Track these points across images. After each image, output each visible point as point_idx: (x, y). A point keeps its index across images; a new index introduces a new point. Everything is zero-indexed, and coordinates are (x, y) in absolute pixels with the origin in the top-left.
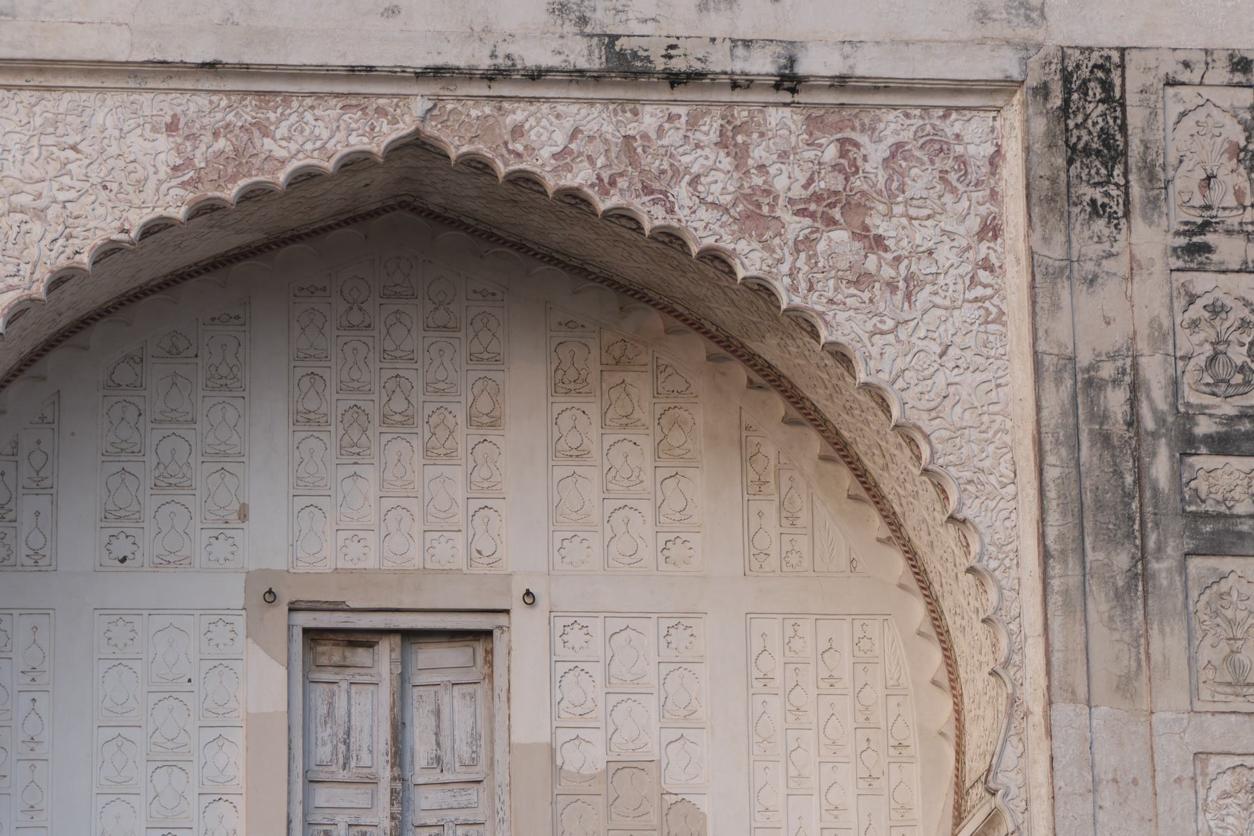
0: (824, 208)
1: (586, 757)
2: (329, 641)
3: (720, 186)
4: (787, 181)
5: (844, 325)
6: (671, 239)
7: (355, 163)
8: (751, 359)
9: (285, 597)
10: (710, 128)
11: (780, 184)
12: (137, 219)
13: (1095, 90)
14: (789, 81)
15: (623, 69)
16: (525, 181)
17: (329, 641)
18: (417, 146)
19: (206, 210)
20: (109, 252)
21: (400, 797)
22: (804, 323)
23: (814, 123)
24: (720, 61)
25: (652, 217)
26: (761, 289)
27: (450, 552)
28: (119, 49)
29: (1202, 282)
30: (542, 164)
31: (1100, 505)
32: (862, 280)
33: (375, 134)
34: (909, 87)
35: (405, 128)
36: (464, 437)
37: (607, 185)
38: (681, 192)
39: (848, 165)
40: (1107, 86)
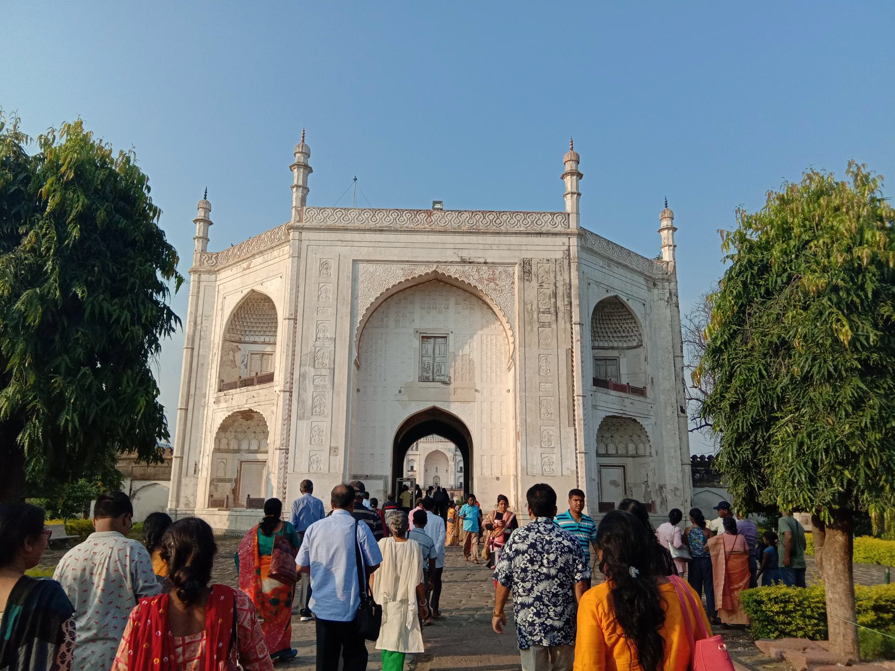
0: (492, 280)
2: (425, 338)
3: (476, 277)
6: (470, 284)
7: (427, 274)
10: (475, 268)
14: (486, 263)
15: (463, 262)
16: (450, 276)
17: (425, 338)
18: (435, 271)
20: (394, 286)
21: (434, 359)
24: (476, 260)
25: (467, 281)
28: (395, 259)
34: (502, 264)
36: (444, 310)
39: (494, 274)
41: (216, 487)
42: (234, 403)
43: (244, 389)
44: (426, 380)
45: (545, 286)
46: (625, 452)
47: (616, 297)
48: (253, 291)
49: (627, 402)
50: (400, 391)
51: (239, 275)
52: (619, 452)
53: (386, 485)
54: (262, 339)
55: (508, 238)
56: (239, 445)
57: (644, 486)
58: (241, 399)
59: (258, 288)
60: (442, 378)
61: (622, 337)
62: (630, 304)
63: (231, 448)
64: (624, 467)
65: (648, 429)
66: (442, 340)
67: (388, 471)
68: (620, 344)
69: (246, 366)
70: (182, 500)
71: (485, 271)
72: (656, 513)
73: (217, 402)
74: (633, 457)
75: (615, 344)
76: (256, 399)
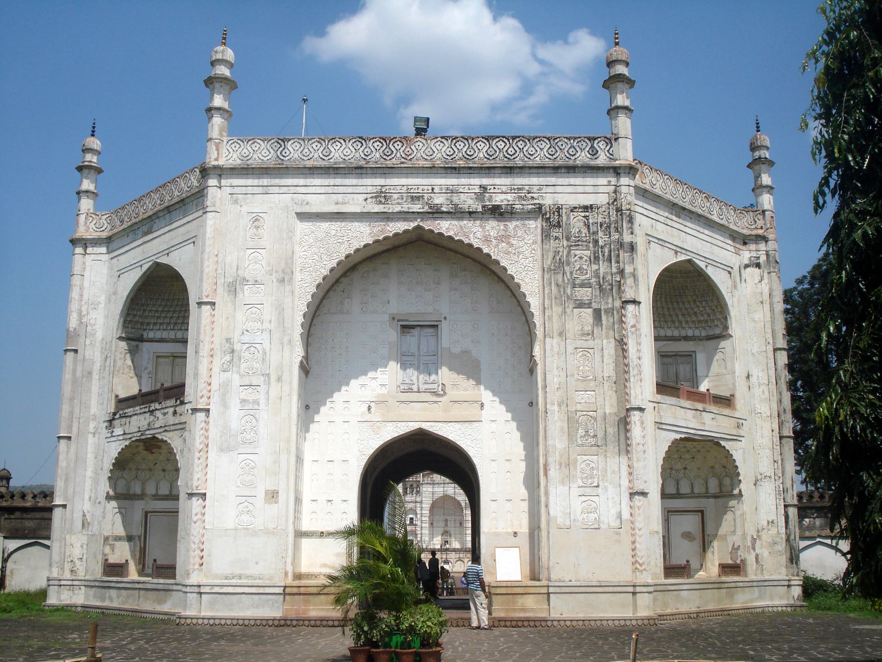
1: (456, 350)
3: (479, 235)
5: (503, 263)
7: (406, 232)
9: (397, 318)
11: (492, 234)
12: (362, 244)
13: (556, 214)
16: (441, 234)
18: (418, 228)
19: (377, 242)
20: (357, 251)
22: (497, 262)
25: (466, 241)
26: (489, 255)
27: (430, 309)
30: (443, 231)
31: (556, 298)
32: (508, 253)
33: (411, 225)
35: (416, 224)
37: (457, 235)
38: (471, 236)
39: (506, 230)
40: (559, 212)
46: (703, 490)
47: (689, 261)
50: (369, 408)
52: (696, 491)
56: (143, 489)
58: (138, 423)
59: (164, 260)
61: (700, 322)
62: (710, 271)
63: (132, 492)
64: (702, 512)
65: (737, 456)
66: (430, 331)
68: (697, 333)
71: (493, 227)
72: (746, 576)
74: (715, 497)
75: (690, 333)
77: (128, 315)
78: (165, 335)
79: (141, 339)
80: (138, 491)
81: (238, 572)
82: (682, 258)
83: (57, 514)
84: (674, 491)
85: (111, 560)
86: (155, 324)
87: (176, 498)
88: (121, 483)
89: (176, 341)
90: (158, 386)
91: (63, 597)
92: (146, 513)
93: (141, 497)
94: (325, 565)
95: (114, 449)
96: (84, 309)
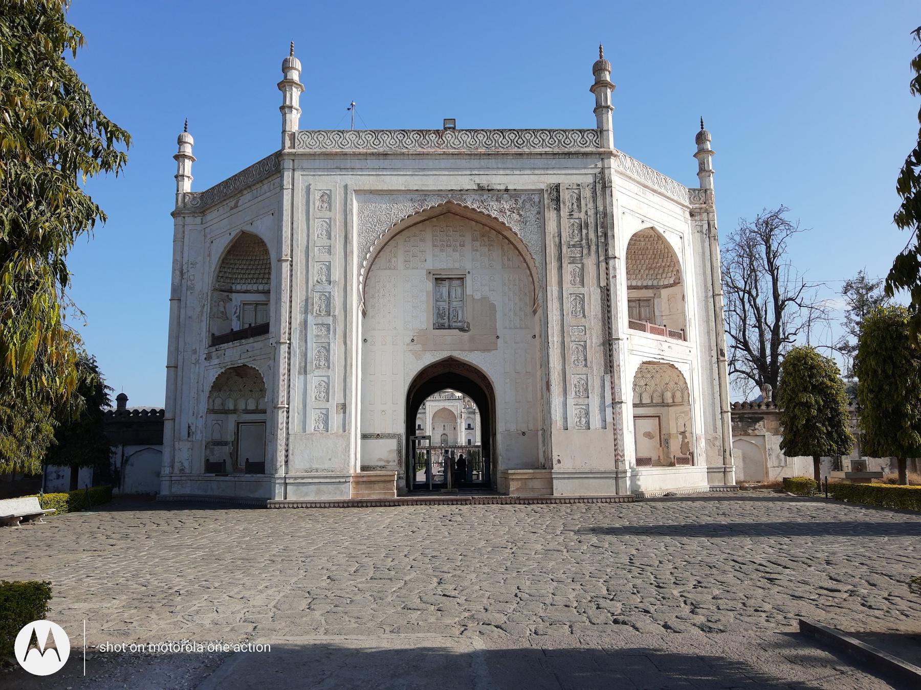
1: (478, 296)
2: (439, 280)
4: (507, 207)
6: (489, 216)
8: (502, 235)
10: (495, 198)
23: (511, 197)
25: (486, 212)
26: (503, 223)
27: (457, 265)
29: (572, 221)
41: (212, 451)
42: (227, 359)
43: (237, 343)
44: (440, 327)
45: (576, 215)
48: (243, 232)
49: (665, 345)
50: (413, 340)
51: (225, 216)
53: (399, 444)
54: (255, 287)
55: (532, 161)
57: (680, 437)
58: (233, 354)
59: (248, 228)
60: (459, 324)
62: (667, 236)
63: (226, 408)
64: (659, 417)
66: (458, 282)
67: (401, 429)
69: (238, 317)
70: (177, 466)
73: (208, 358)
76: (250, 354)
77: (220, 271)
78: (250, 287)
79: (231, 291)
80: (231, 407)
81: (315, 466)
82: (647, 225)
83: (168, 426)
84: (648, 401)
85: (211, 461)
86: (241, 279)
87: (265, 412)
88: (218, 401)
89: (258, 292)
90: (247, 326)
91: (173, 490)
92: (238, 423)
93: (234, 411)
94: (380, 460)
95: (213, 375)
96: (185, 267)
